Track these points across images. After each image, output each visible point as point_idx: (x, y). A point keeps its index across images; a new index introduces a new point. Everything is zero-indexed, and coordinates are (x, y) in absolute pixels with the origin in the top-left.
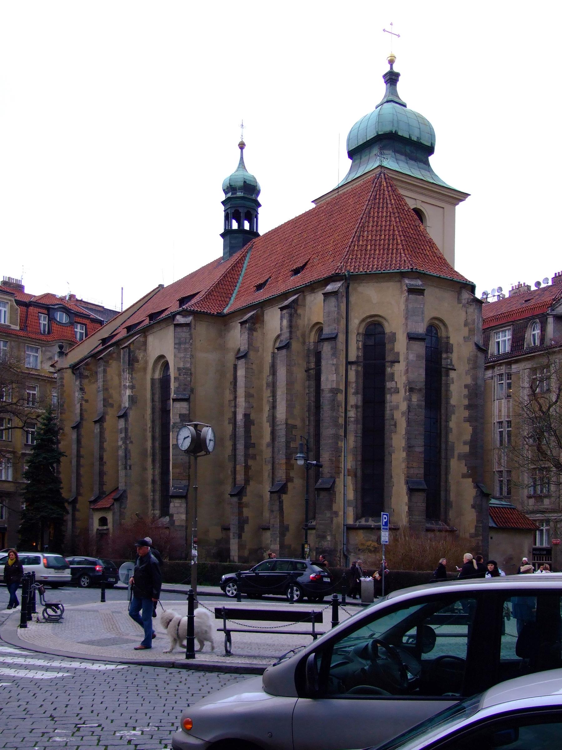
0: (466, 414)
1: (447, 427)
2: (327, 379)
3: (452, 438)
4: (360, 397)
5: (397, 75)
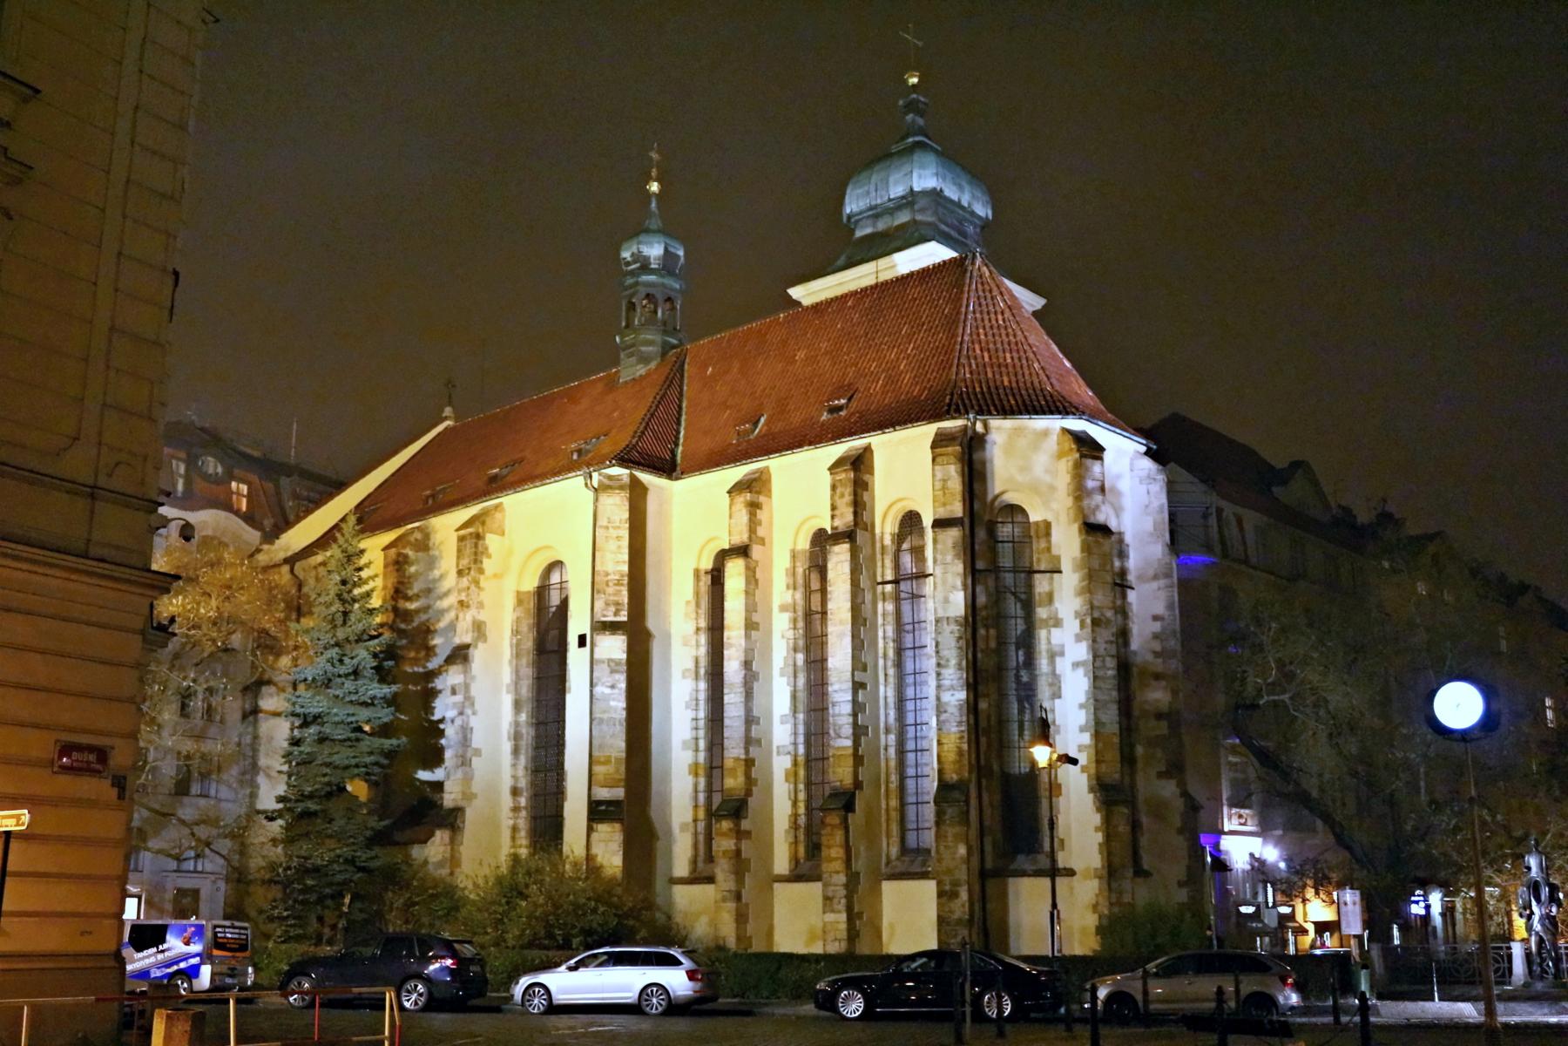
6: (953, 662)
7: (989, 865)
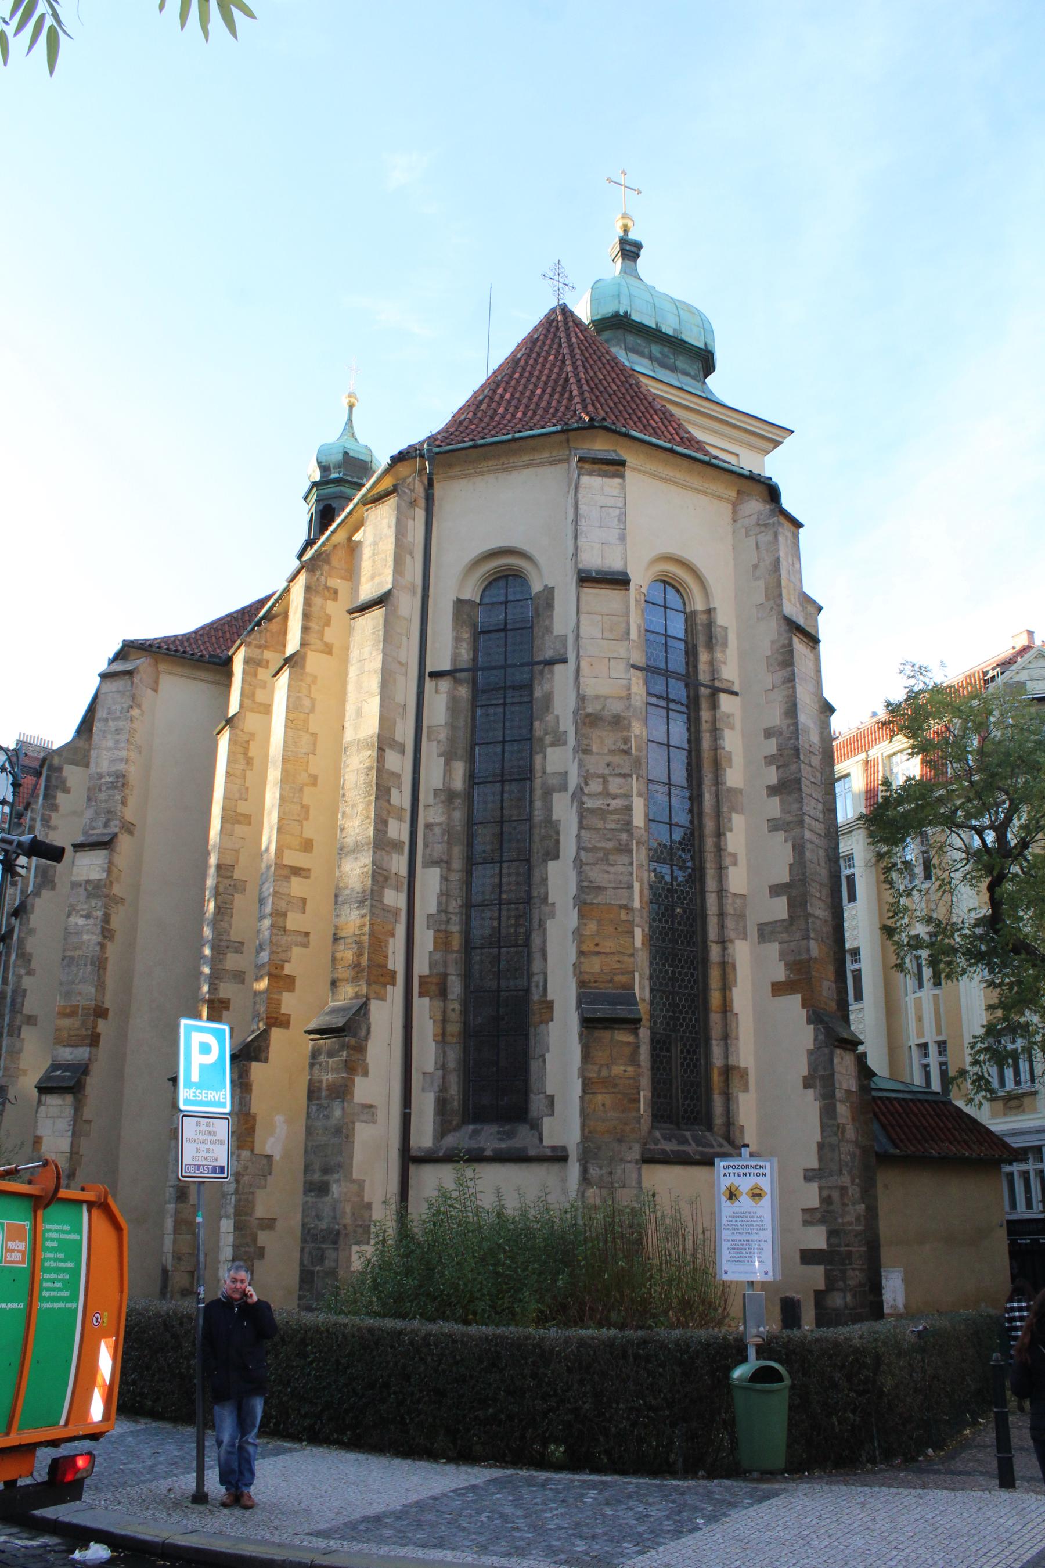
0: (774, 807)
1: (719, 849)
2: (359, 713)
3: (737, 880)
4: (459, 769)
5: (638, 246)
6: (360, 807)
7: (424, 1138)
